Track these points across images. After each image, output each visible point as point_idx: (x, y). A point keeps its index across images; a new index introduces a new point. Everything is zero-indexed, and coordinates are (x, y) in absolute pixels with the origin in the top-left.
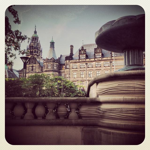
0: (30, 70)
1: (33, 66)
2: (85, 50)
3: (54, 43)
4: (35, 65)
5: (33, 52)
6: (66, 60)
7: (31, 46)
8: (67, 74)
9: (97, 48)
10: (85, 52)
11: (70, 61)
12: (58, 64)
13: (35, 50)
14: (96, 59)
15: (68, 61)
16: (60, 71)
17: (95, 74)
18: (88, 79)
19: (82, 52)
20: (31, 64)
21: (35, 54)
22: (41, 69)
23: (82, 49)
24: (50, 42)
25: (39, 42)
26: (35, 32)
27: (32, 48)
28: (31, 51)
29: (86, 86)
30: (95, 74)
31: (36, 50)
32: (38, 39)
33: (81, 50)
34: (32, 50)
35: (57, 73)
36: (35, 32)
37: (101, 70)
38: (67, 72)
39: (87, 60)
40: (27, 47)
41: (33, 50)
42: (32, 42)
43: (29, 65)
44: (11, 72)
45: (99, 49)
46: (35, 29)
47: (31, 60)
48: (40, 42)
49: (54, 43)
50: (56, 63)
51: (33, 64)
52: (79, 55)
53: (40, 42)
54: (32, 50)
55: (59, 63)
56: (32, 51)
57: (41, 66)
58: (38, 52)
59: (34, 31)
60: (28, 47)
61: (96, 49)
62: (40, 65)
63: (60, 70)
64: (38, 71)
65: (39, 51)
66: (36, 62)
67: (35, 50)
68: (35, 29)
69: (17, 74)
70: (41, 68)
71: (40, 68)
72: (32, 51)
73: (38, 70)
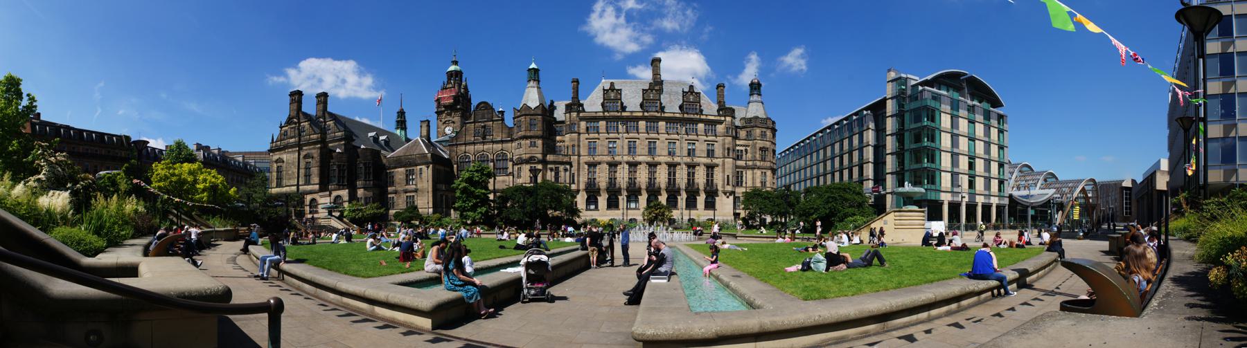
1: (484, 127)
2: (619, 90)
6: (570, 112)
9: (649, 89)
10: (619, 96)
11: (581, 115)
14: (646, 114)
15: (574, 114)
17: (644, 149)
18: (626, 158)
19: (612, 95)
20: (480, 122)
23: (612, 87)
29: (622, 177)
30: (644, 149)
33: (607, 90)
37: (659, 139)
38: (572, 141)
39: (624, 114)
45: (654, 91)
51: (485, 121)
52: (603, 102)
61: (645, 90)
64: (499, 139)
66: (492, 116)
73: (498, 136)
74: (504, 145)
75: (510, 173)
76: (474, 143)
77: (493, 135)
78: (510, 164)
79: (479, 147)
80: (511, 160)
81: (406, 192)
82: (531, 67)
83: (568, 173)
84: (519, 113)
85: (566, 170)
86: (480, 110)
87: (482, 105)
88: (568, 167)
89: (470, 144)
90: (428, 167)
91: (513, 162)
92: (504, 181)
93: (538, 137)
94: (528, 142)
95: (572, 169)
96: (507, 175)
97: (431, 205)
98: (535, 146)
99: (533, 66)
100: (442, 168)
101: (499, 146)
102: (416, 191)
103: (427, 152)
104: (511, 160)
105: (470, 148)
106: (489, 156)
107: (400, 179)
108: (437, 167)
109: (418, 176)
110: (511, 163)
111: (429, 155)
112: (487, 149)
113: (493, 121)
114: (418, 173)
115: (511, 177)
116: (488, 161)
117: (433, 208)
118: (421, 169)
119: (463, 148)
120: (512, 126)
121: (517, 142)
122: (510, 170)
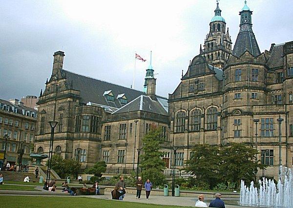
1: (197, 82)
3: (251, 13)
4: (204, 77)
5: (214, 59)
7: (209, 44)
8: (288, 92)
12: (262, 67)
13: (217, 52)
16: (270, 87)
21: (218, 61)
24: (240, 13)
26: (218, 12)
27: (212, 49)
32: (224, 26)
35: (261, 93)
36: (218, 12)
42: (212, 34)
43: (188, 80)
46: (218, 4)
49: (251, 13)
50: (257, 66)
55: (265, 66)
56: (212, 54)
57: (218, 79)
59: (215, 8)
60: (203, 48)
62: (216, 77)
63: (268, 84)
67: (217, 52)
68: (218, 4)
69: (164, 104)
70: (217, 82)
71: (216, 84)
72: (212, 54)
74: (214, 100)
79: (192, 102)
81: (118, 145)
83: (283, 124)
85: (280, 121)
88: (283, 117)
91: (221, 116)
92: (213, 137)
95: (290, 119)
102: (126, 145)
104: (219, 114)
105: (185, 104)
107: (115, 133)
109: (129, 131)
110: (219, 118)
112: (200, 105)
114: (129, 127)
118: (131, 124)
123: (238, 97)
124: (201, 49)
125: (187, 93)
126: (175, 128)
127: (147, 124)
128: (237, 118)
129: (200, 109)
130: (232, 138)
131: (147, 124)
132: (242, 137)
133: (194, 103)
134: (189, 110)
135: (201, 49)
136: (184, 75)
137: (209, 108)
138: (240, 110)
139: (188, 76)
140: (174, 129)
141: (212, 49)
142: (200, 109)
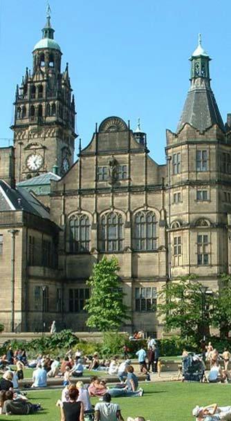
0: (103, 180)
4: (127, 156)
22: (158, 175)
25: (63, 70)
27: (40, 96)
28: (32, 108)
31: (54, 105)
32: (59, 60)
34: (36, 105)
36: (49, 33)
40: (18, 90)
41: (44, 104)
44: (12, 190)
46: (49, 18)
47: (100, 135)
48: (67, 69)
53: (67, 69)
54: (36, 105)
56: (40, 107)
58: (62, 110)
59: (44, 25)
65: (67, 108)
75: (161, 248)
76: (97, 191)
77: (130, 179)
78: (160, 231)
79: (105, 199)
80: (164, 224)
82: (196, 54)
84: (176, 140)
86: (107, 132)
87: (111, 123)
89: (89, 192)
90: (15, 233)
93: (210, 183)
94: (194, 191)
96: (156, 251)
97: (18, 306)
98: (205, 199)
99: (199, 52)
100: (38, 235)
101: (139, 200)
103: (13, 208)
105: (89, 201)
106: (123, 215)
108: (32, 233)
110: (162, 230)
111: (19, 214)
112: (120, 204)
113: (130, 151)
115: (163, 254)
116: (120, 225)
117: (22, 311)
119: (75, 200)
120: (164, 163)
121: (173, 192)
122: (161, 242)
123: (201, 197)
124: (17, 93)
125: (91, 181)
126: (68, 244)
127: (30, 237)
128: (202, 234)
129: (120, 212)
130: (195, 266)
131: (30, 237)
132: (211, 266)
133: (106, 201)
134: (99, 212)
135: (17, 93)
136: (83, 148)
137: (140, 212)
138: (209, 220)
139: (93, 150)
140: (65, 244)
141: (40, 96)
142: (120, 212)
